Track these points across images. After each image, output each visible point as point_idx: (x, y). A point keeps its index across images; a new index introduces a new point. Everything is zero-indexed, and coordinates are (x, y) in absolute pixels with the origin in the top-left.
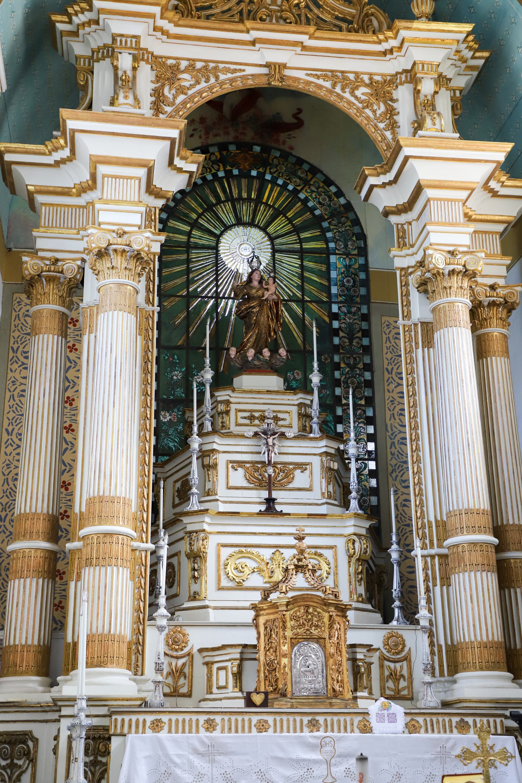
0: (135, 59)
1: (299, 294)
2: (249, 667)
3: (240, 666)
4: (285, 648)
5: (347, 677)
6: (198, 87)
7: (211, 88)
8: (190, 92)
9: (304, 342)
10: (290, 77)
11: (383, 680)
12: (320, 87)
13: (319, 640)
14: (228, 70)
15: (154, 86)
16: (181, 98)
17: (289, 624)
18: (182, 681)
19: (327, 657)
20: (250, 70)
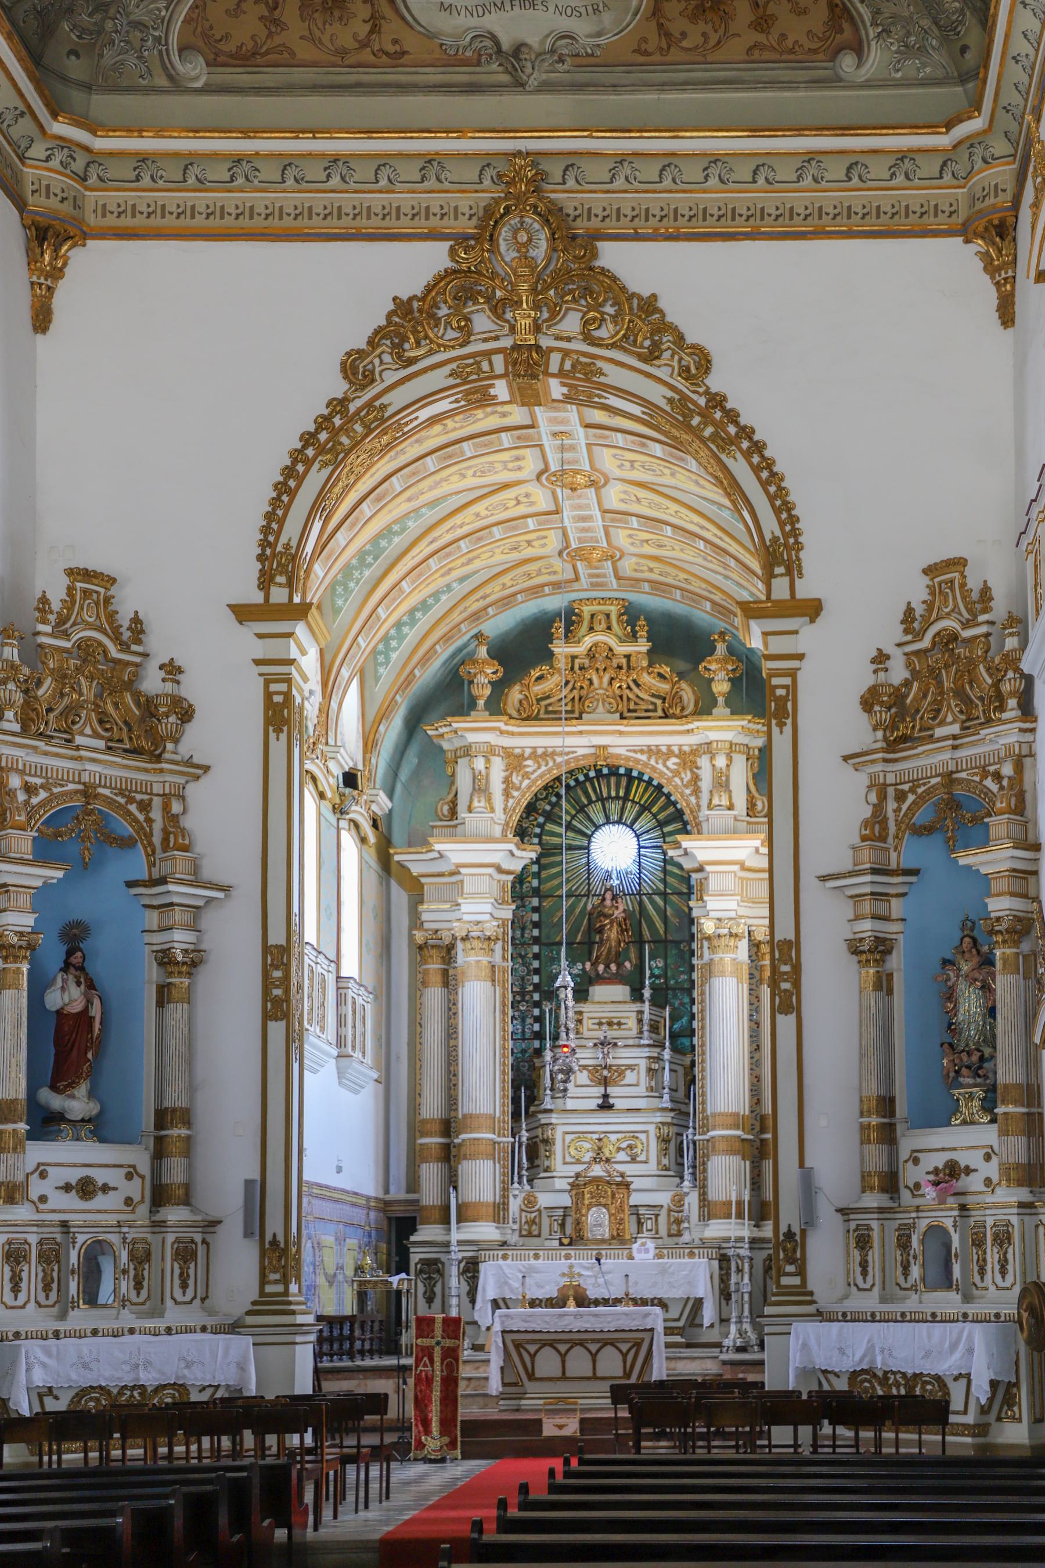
0: (488, 761)
1: (661, 887)
2: (569, 1221)
3: (564, 1220)
4: (584, 1211)
5: (631, 1226)
6: (539, 771)
7: (550, 771)
8: (533, 777)
9: (665, 932)
10: (612, 755)
11: (669, 1224)
12: (637, 761)
13: (605, 1206)
14: (561, 754)
15: (504, 774)
16: (526, 782)
17: (587, 1196)
18: (534, 1227)
19: (611, 1215)
20: (581, 752)
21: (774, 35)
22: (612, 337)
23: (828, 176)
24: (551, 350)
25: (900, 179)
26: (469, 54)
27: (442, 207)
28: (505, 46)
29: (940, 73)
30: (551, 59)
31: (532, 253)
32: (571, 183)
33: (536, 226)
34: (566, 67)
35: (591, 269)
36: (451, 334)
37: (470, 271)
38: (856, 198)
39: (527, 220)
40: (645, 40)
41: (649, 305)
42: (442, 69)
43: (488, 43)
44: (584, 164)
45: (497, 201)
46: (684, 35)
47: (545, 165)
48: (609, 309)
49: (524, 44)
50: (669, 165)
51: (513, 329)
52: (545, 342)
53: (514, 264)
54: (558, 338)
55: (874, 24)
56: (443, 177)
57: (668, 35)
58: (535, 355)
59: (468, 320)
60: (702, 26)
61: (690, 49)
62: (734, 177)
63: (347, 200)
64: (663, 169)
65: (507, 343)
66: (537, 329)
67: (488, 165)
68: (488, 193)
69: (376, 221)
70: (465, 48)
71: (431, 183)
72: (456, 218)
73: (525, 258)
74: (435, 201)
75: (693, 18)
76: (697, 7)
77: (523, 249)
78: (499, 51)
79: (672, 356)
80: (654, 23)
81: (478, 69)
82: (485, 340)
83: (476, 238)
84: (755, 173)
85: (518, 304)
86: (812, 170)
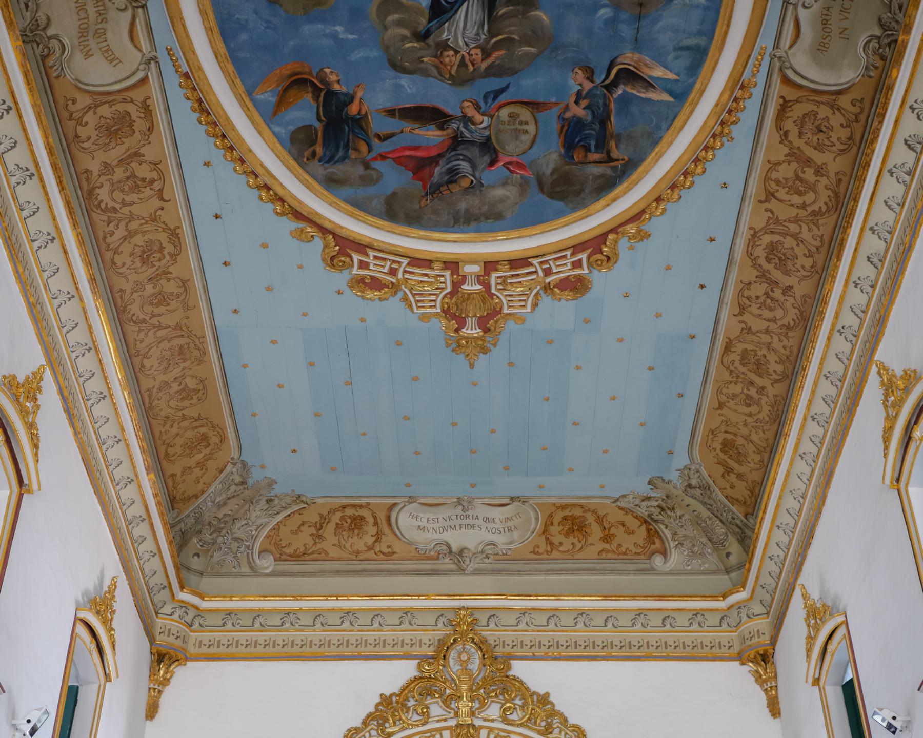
21: (614, 546)
22: (521, 719)
23: (651, 624)
24: (481, 727)
25: (695, 627)
26: (432, 553)
27: (412, 640)
28: (455, 548)
29: (714, 568)
30: (481, 556)
31: (470, 667)
32: (492, 626)
33: (473, 650)
34: (490, 560)
35: (507, 677)
36: (416, 717)
37: (430, 678)
38: (671, 637)
39: (467, 647)
40: (538, 547)
41: (544, 700)
42: (415, 562)
43: (445, 548)
44: (501, 615)
45: (448, 636)
46: (561, 544)
47: (477, 615)
48: (518, 702)
49: (465, 548)
50: (553, 616)
51: (456, 714)
52: (477, 722)
53: (459, 673)
54: (485, 720)
55: (673, 540)
56: (413, 623)
57: (551, 544)
58: (471, 731)
59: (428, 708)
60: (572, 539)
61: (564, 552)
62: (593, 623)
63: (353, 636)
64: (549, 618)
65: (453, 723)
66: (472, 714)
67: (442, 615)
68: (442, 631)
69: (370, 648)
70: (430, 550)
71: (406, 625)
72: (420, 646)
73: (465, 670)
74: (408, 636)
75: (567, 535)
76: (569, 529)
77: (464, 665)
78: (451, 552)
79: (560, 732)
80: (543, 538)
81: (437, 562)
82: (438, 721)
83: (433, 658)
84: (606, 621)
85: (460, 698)
86: (641, 620)
